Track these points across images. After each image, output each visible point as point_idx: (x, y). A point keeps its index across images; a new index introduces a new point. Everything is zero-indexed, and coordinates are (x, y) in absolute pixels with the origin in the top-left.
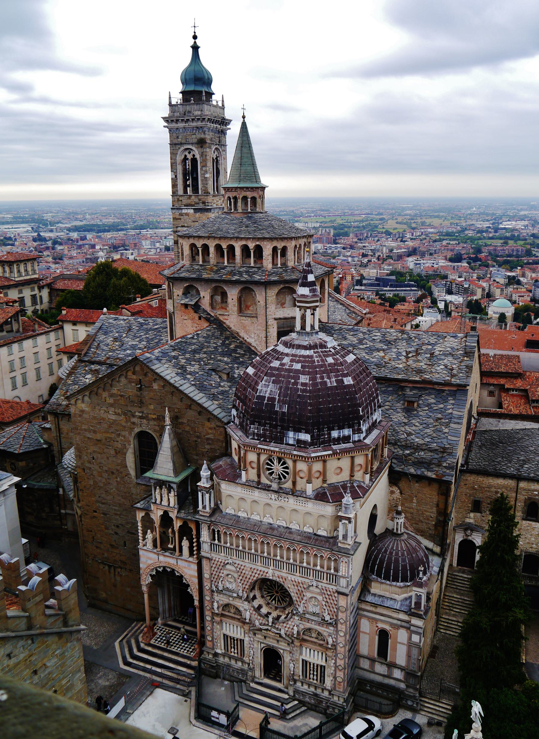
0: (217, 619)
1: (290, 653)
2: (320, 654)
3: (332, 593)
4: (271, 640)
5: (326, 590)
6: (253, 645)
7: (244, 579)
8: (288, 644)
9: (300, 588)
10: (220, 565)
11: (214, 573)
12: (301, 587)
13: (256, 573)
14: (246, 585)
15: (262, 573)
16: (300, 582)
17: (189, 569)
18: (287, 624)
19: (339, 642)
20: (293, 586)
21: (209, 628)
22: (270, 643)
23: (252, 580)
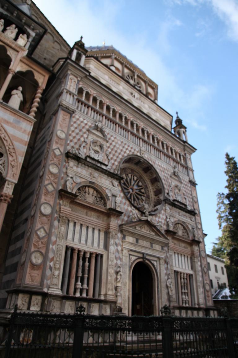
0: (66, 208)
2: (186, 258)
6: (121, 259)
9: (166, 175)
10: (83, 127)
11: (74, 134)
13: (127, 149)
14: (115, 160)
15: (133, 151)
17: (14, 127)
21: (41, 233)
22: (143, 251)
23: (123, 156)
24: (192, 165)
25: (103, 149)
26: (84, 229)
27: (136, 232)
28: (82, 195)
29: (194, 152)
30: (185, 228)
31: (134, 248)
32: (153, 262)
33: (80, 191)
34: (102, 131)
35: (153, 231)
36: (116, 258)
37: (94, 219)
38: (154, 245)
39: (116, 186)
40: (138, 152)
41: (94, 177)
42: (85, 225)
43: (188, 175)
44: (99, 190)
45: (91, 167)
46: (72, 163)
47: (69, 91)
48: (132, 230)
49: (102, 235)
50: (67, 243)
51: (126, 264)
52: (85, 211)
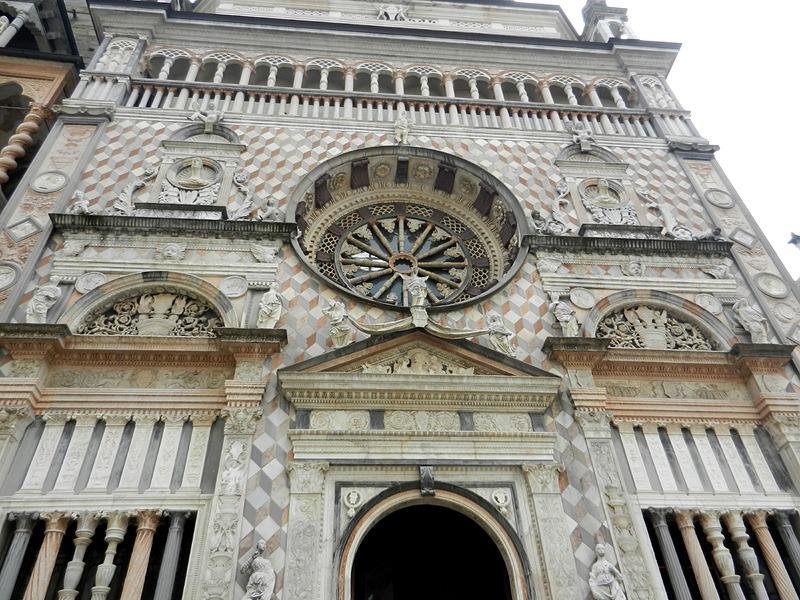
1: (563, 476)
2: (727, 444)
3: (658, 162)
4: (422, 422)
5: (632, 156)
6: (278, 514)
7: (268, 169)
8: (537, 419)
9: (529, 165)
10: (148, 142)
11: (104, 169)
12: (533, 161)
13: (331, 146)
14: (277, 188)
16: (524, 144)
18: (506, 308)
19: (784, 329)
20: (500, 164)
22: (414, 452)
24: (674, 99)
25: (218, 176)
26: (113, 436)
27: (356, 386)
28: (122, 326)
29: (676, 54)
30: (680, 317)
31: (359, 449)
32: (484, 493)
33: (112, 317)
34: (219, 129)
35: (466, 363)
36: (250, 513)
37: (171, 391)
38: (478, 419)
39: (270, 256)
40: (383, 139)
41: (165, 259)
42: (115, 419)
43: (659, 135)
44: (192, 289)
45: (153, 232)
46: (72, 244)
47: (99, 74)
48: (329, 381)
49: (201, 437)
50: (12, 505)
51: (310, 530)
52: (129, 372)
